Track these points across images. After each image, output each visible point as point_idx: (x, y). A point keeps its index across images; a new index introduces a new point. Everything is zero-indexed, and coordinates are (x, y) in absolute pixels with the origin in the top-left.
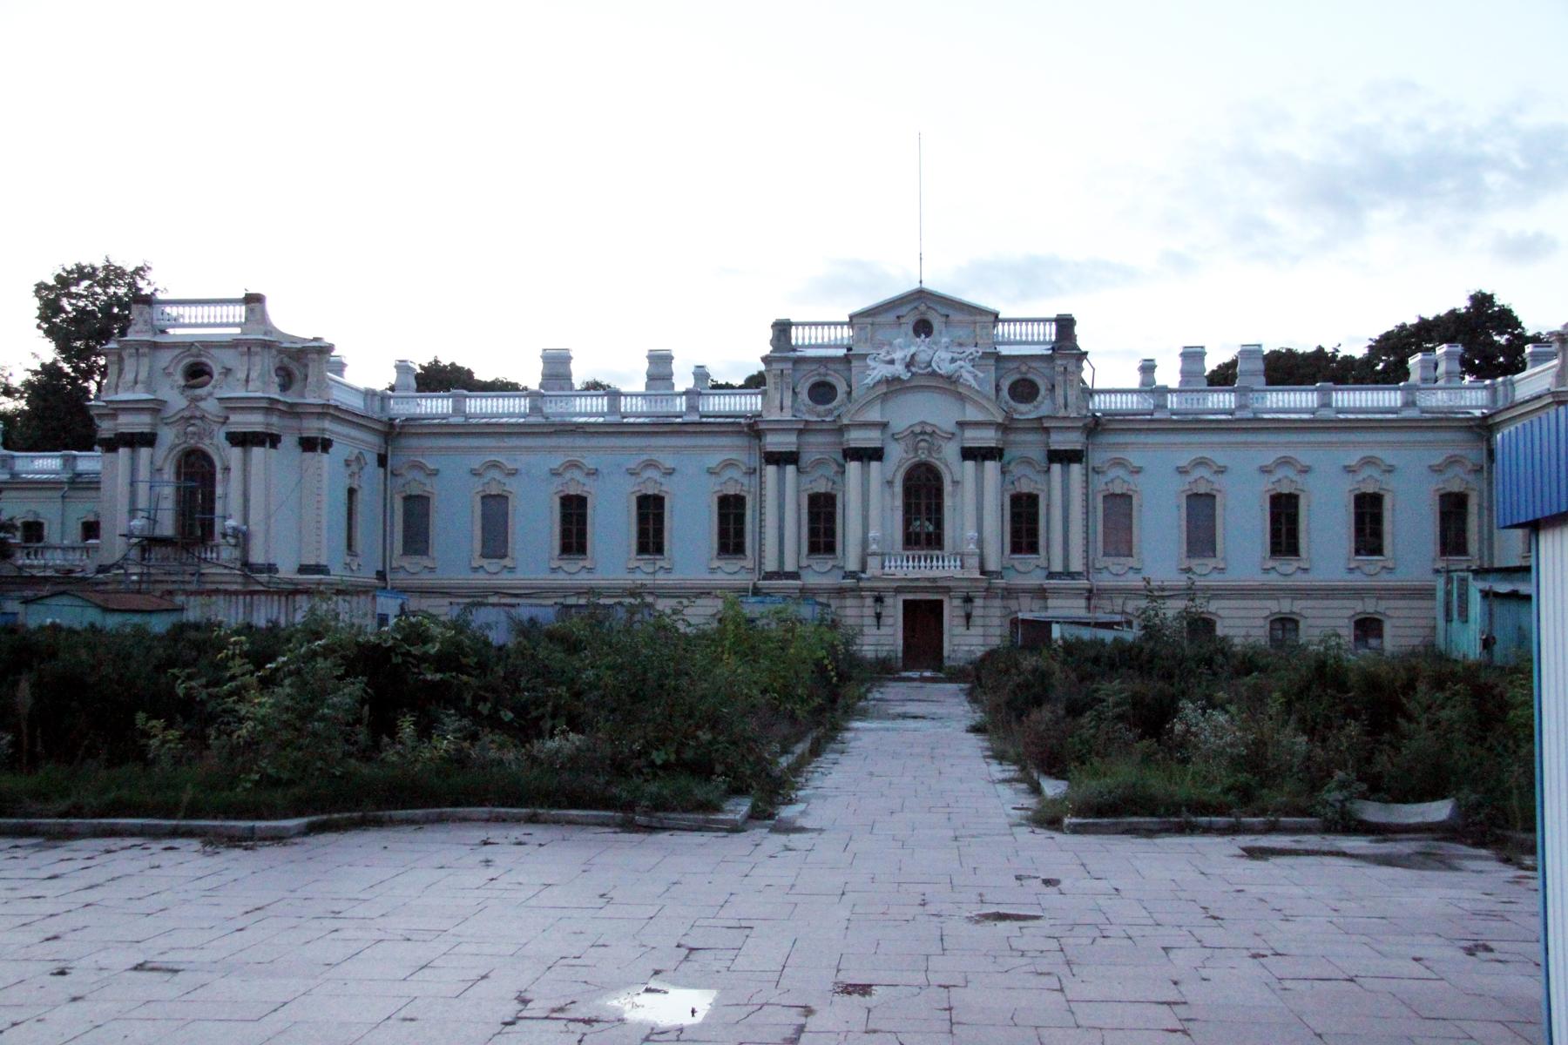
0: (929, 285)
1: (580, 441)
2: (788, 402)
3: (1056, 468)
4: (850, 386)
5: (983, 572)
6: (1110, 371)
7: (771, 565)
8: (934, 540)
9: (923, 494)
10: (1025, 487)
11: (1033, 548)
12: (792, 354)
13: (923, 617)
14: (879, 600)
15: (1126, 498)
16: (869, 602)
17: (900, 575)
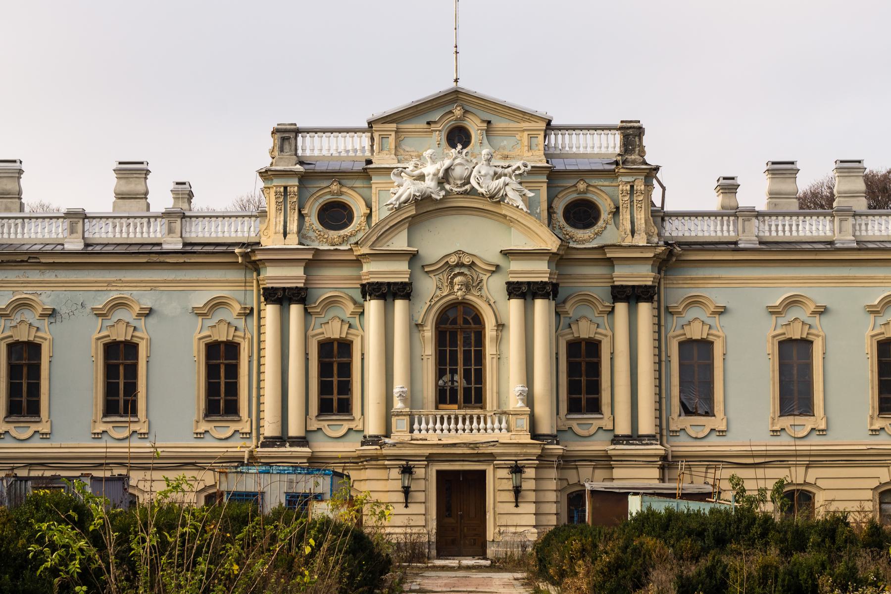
0: (465, 85)
1: (34, 275)
2: (293, 226)
3: (621, 308)
5: (534, 436)
6: (686, 189)
7: (270, 429)
8: (474, 396)
9: (459, 342)
10: (584, 331)
11: (595, 407)
12: (299, 168)
13: (460, 494)
14: (407, 470)
15: (706, 345)
16: (395, 473)
17: (432, 438)
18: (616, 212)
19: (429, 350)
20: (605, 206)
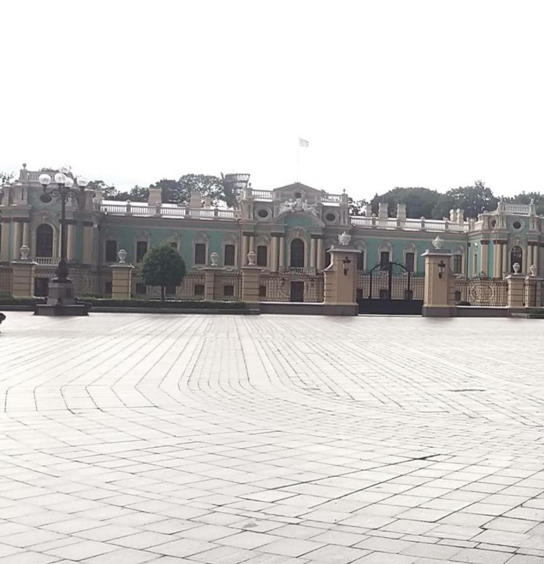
4: (273, 211)
18: (340, 218)
19: (289, 251)
20: (337, 215)
